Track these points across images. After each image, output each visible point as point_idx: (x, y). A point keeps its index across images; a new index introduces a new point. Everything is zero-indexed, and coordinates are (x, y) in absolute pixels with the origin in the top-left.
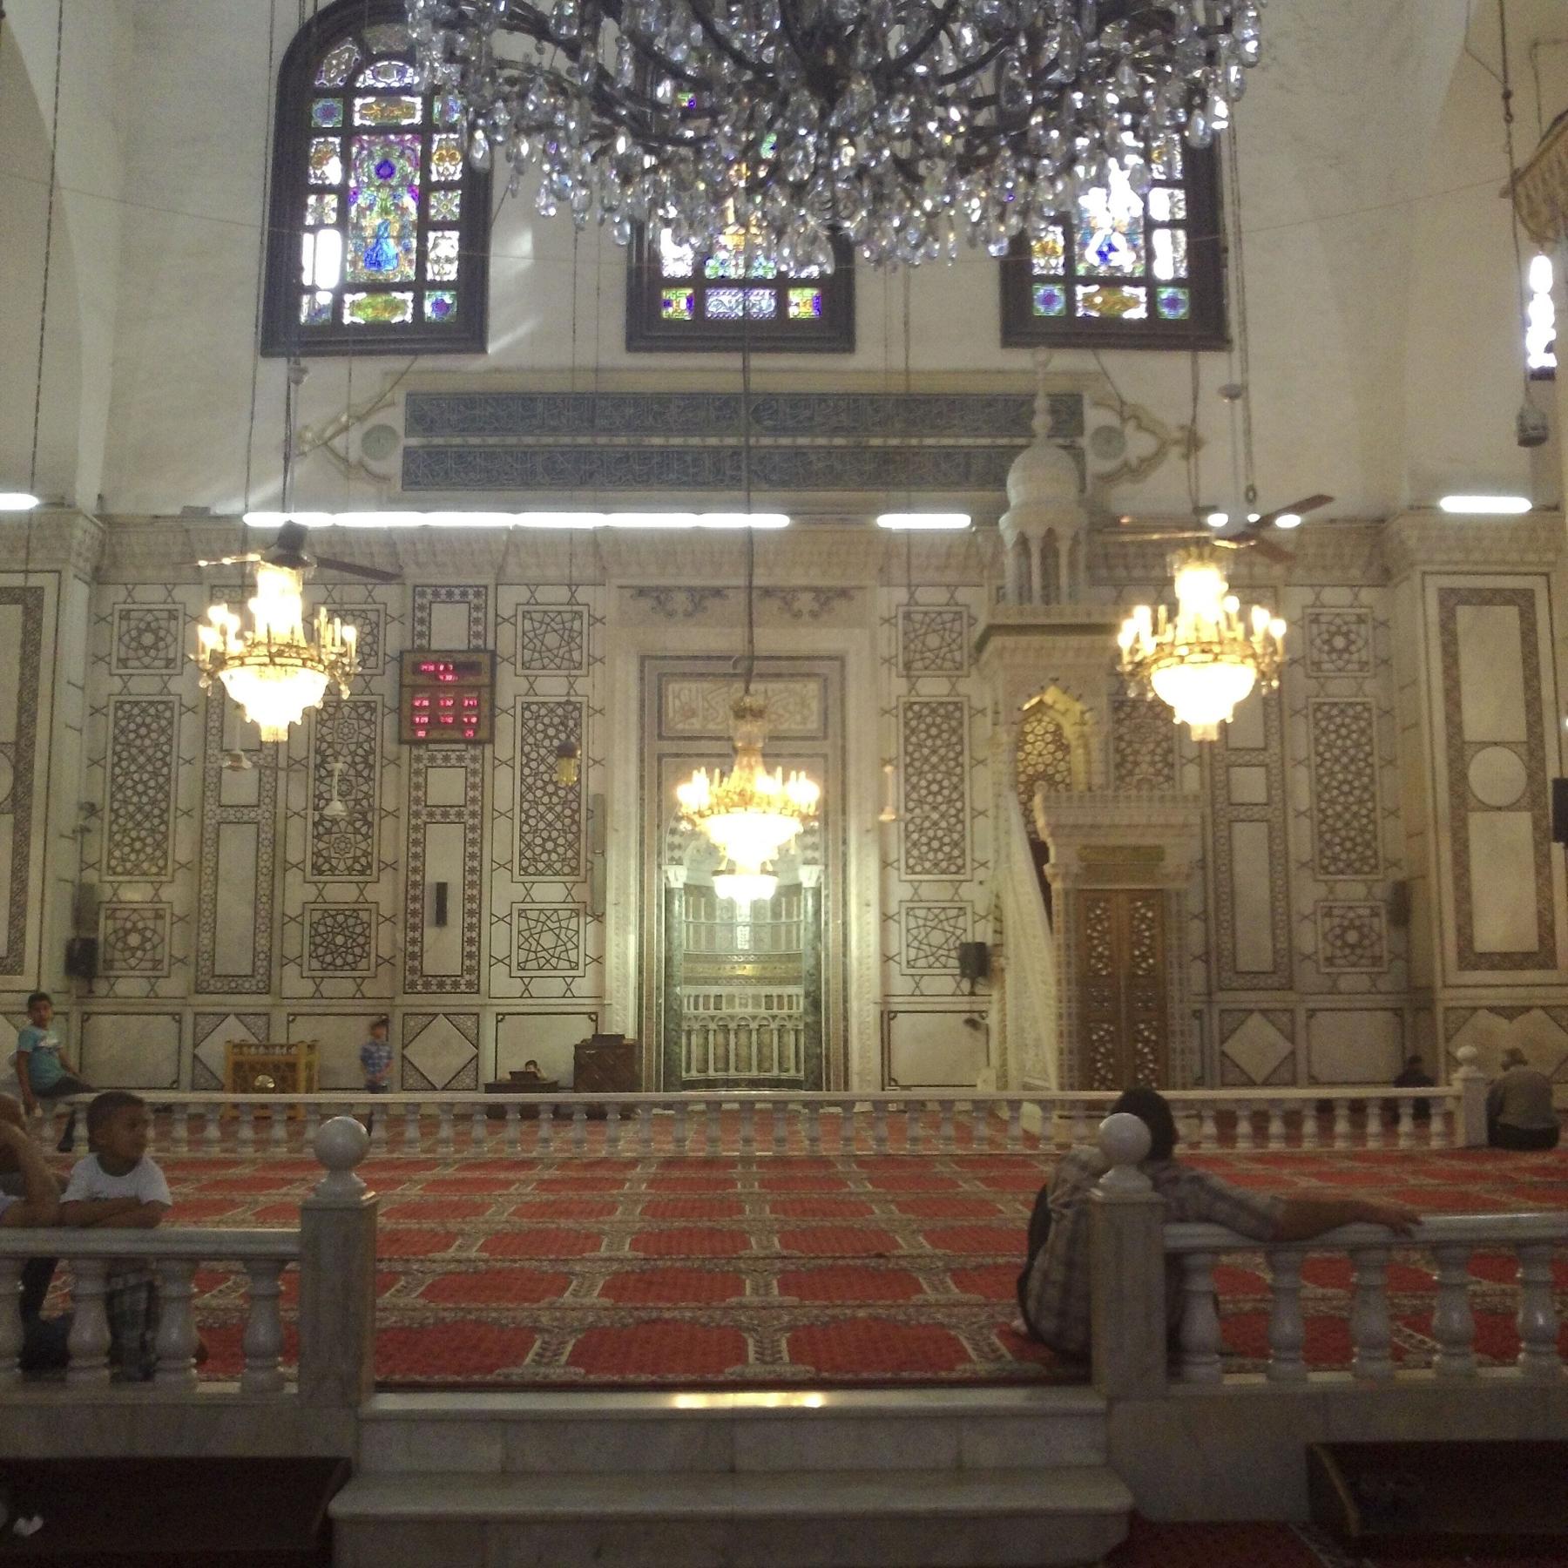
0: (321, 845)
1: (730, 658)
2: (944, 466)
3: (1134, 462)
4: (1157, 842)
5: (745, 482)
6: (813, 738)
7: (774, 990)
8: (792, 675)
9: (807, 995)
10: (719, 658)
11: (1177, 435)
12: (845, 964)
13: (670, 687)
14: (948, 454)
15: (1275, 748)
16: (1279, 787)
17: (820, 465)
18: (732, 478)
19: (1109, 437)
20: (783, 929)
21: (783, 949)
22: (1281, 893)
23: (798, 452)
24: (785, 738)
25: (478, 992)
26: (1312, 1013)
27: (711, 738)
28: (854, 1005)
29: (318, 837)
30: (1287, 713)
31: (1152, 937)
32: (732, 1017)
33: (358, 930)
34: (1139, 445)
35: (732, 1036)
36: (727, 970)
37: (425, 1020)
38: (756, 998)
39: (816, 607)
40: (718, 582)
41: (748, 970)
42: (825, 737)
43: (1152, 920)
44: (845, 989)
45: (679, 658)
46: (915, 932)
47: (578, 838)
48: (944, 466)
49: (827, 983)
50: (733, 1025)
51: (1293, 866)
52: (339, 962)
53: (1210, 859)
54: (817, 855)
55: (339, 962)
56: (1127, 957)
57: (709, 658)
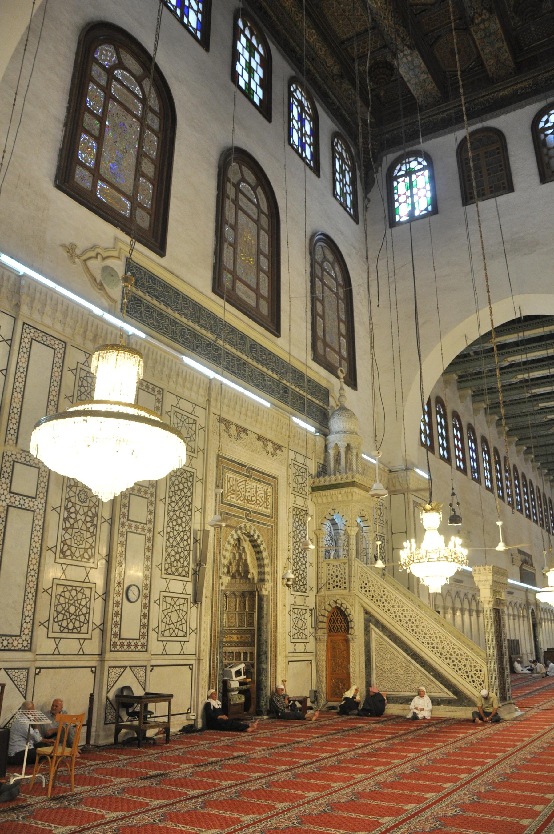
0: (67, 536)
1: (245, 466)
6: (268, 517)
13: (227, 474)
23: (262, 374)
25: (146, 651)
27: (239, 508)
29: (65, 529)
33: (83, 602)
37: (120, 670)
45: (229, 460)
47: (189, 554)
52: (71, 626)
55: (71, 626)
57: (239, 464)
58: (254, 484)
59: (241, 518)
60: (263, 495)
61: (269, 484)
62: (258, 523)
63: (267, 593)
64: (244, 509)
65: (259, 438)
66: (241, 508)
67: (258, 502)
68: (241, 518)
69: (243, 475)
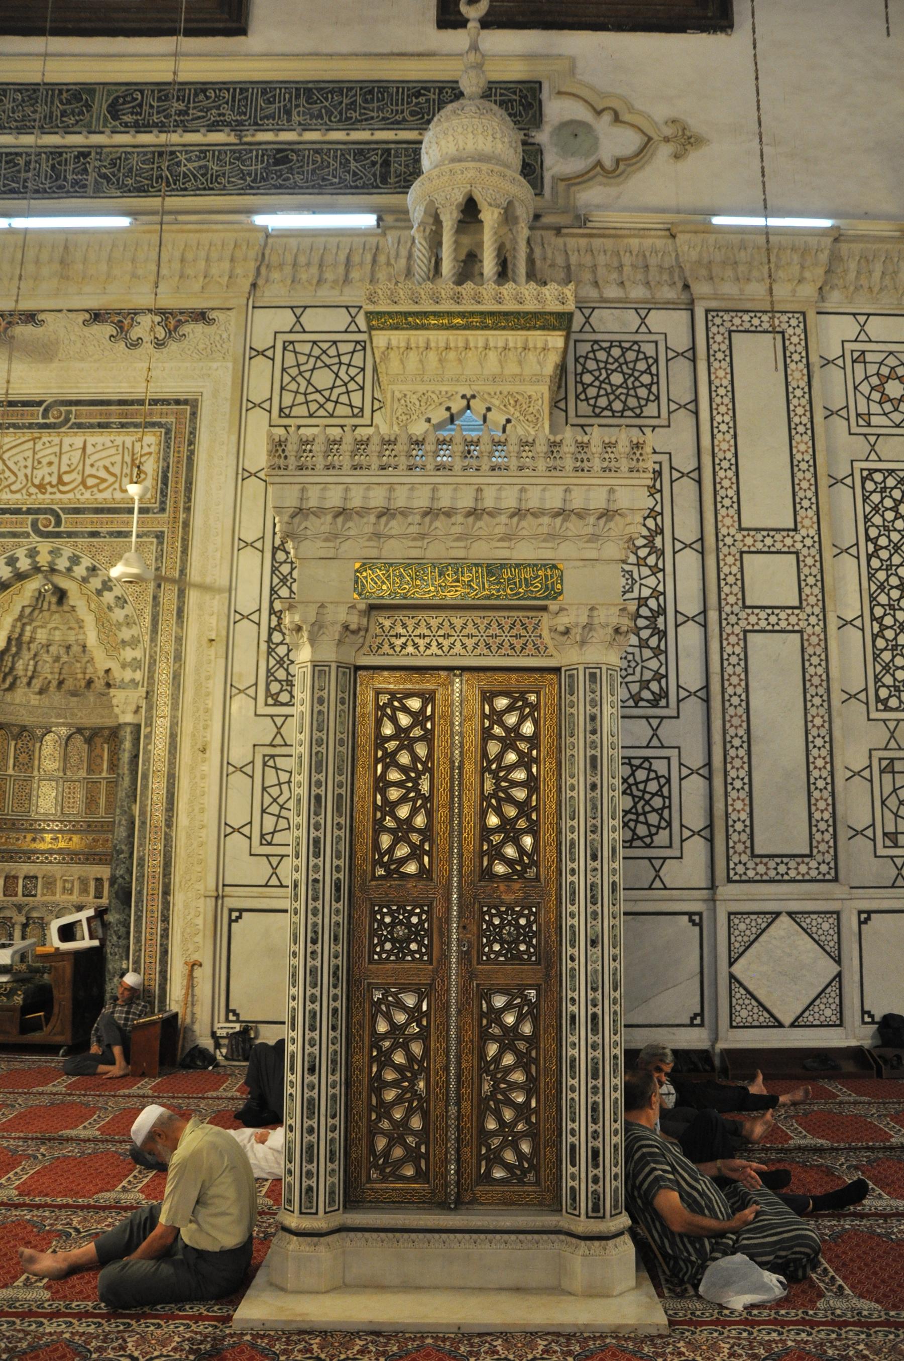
2: (353, 165)
3: (608, 163)
4: (546, 553)
5: (90, 190)
8: (123, 426)
9: (113, 881)
10: (25, 404)
11: (668, 131)
12: (168, 838)
14: (361, 151)
15: (808, 528)
16: (815, 585)
17: (190, 166)
18: (75, 183)
19: (574, 133)
22: (819, 739)
24: (110, 511)
26: (864, 917)
28: (179, 899)
30: (823, 482)
31: (532, 784)
34: (615, 142)
39: (161, 333)
40: (26, 305)
42: (163, 510)
43: (534, 740)
44: (167, 874)
46: (275, 791)
48: (353, 165)
49: (141, 865)
51: (837, 698)
53: (715, 687)
54: (138, 676)
56: (470, 832)
58: (78, 441)
59: (14, 535)
60: (118, 458)
61: (153, 425)
62: (94, 534)
63: (129, 718)
64: (29, 511)
65: (97, 316)
66: (18, 511)
67: (91, 482)
68: (14, 535)
69: (30, 426)
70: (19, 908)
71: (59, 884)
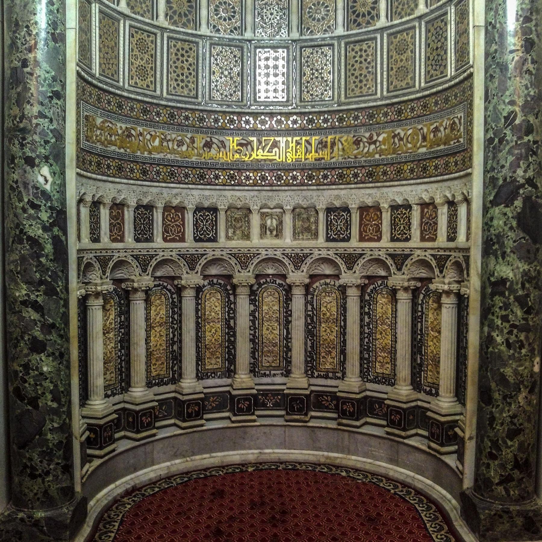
7: (355, 196)
20: (382, 43)
21: (380, 90)
32: (243, 259)
35: (243, 306)
36: (230, 150)
38: (304, 215)
41: (287, 150)
50: (244, 276)
70: (191, 261)
71: (255, 220)
